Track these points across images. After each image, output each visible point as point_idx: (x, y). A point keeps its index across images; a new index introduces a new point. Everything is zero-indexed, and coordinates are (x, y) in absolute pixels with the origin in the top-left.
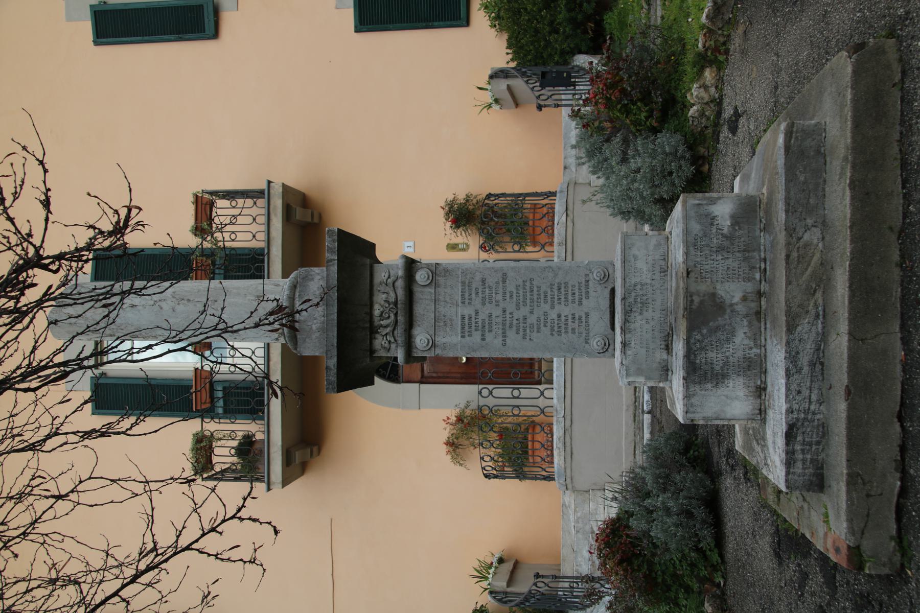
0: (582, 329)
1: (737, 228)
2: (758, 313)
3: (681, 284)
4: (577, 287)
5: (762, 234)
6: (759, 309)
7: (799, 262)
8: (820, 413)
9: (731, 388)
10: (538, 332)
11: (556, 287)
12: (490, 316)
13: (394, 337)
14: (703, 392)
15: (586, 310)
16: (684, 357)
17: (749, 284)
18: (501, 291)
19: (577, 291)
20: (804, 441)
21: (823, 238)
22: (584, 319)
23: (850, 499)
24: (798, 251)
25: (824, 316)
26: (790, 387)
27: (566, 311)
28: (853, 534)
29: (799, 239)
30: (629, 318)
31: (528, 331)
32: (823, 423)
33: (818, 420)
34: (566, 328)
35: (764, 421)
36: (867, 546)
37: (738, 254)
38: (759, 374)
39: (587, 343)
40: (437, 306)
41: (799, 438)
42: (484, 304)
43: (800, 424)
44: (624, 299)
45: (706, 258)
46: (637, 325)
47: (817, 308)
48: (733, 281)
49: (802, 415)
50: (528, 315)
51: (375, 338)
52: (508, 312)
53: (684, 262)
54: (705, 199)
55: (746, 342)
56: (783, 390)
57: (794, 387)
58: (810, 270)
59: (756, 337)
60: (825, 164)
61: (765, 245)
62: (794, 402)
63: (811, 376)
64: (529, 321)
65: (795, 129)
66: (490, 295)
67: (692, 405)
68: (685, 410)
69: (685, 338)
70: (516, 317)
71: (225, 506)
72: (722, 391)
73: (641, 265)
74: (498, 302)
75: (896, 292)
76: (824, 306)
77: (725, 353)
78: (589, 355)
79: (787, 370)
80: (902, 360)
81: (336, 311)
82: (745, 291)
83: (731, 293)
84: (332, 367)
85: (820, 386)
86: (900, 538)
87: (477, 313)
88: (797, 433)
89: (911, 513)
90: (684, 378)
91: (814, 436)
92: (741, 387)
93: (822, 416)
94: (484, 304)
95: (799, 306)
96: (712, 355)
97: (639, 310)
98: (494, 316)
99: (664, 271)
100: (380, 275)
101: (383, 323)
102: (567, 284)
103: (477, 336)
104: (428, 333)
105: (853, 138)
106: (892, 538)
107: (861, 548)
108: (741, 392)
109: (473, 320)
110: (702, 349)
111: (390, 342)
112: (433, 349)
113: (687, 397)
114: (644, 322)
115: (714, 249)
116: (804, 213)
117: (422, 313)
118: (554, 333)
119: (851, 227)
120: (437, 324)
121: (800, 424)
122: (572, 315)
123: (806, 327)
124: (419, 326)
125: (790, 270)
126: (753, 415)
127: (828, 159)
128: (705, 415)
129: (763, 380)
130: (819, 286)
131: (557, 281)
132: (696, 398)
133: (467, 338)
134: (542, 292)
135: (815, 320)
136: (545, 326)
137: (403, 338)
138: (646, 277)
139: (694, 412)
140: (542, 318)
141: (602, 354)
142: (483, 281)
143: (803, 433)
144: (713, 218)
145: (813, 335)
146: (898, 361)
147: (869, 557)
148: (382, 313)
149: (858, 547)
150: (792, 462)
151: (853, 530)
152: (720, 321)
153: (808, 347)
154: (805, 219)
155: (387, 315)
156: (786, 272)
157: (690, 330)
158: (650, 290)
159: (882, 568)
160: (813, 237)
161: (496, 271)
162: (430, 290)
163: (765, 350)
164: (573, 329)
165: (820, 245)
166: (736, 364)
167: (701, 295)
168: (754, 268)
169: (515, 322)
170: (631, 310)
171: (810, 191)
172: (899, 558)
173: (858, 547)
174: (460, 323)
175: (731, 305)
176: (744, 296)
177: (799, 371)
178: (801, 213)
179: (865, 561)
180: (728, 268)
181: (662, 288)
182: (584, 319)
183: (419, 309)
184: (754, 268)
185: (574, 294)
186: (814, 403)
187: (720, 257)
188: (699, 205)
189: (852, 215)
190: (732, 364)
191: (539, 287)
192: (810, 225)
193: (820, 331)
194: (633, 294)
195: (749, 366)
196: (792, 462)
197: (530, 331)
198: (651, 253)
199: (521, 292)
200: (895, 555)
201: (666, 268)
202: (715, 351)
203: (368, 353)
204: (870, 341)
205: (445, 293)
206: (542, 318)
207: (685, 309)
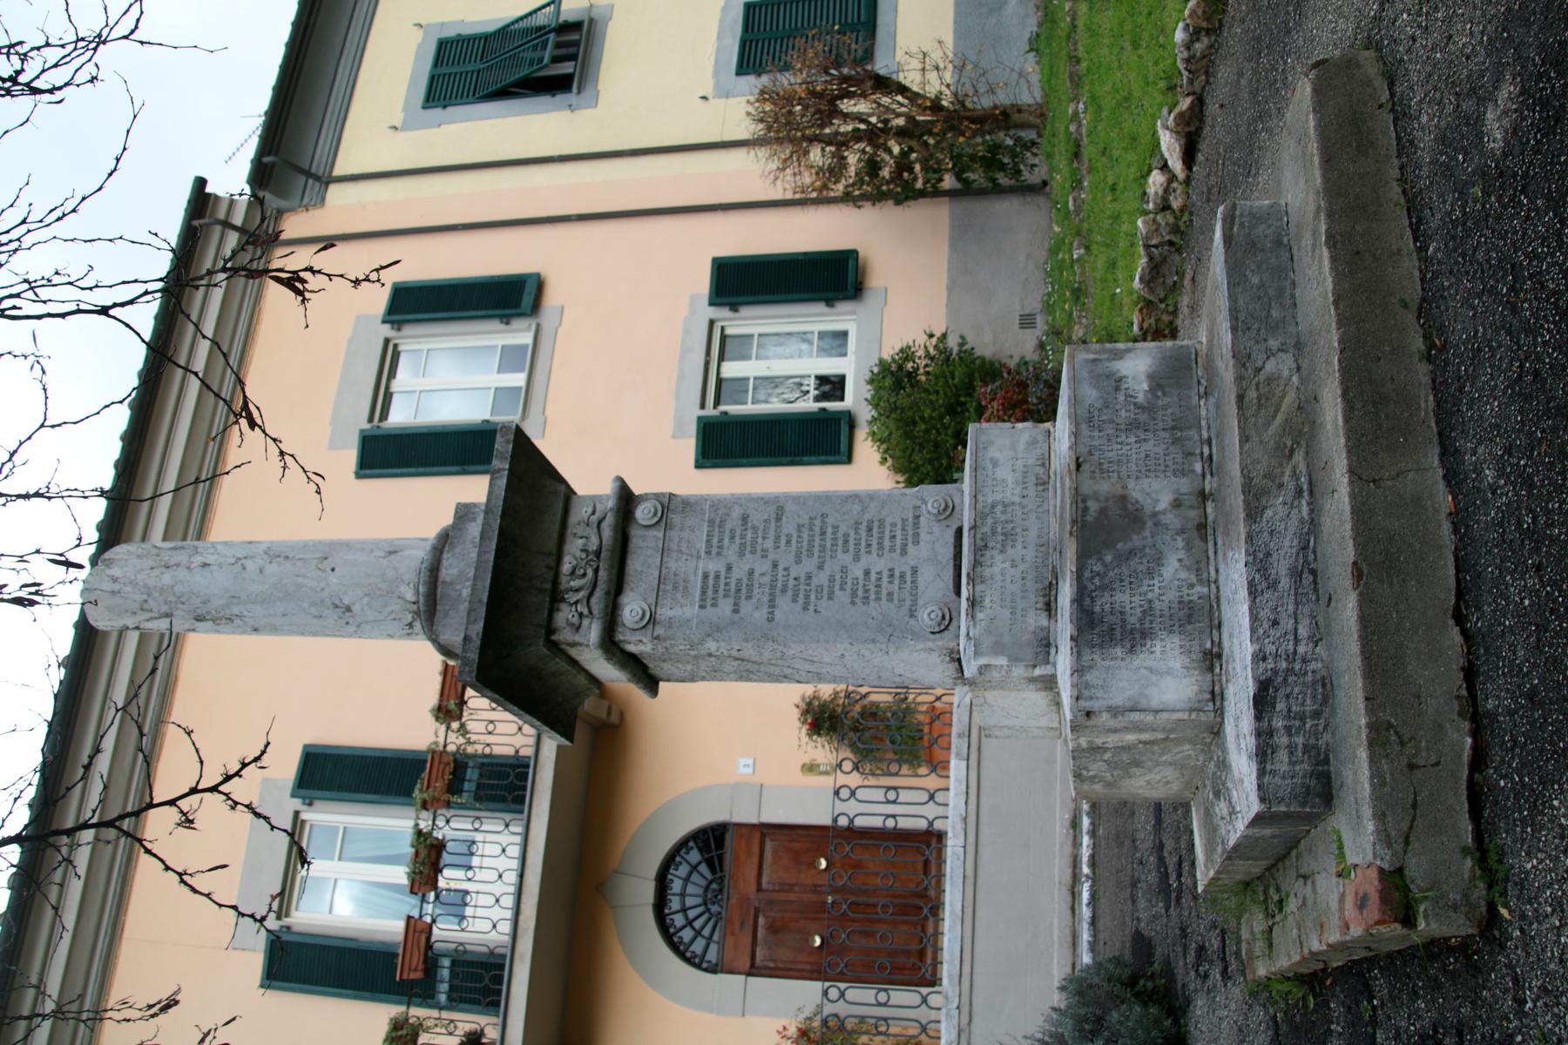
0: (906, 594)
1: (1159, 394)
2: (1202, 527)
3: (1068, 483)
4: (899, 526)
5: (1202, 403)
6: (1203, 520)
7: (1260, 406)
8: (1316, 659)
9: (1158, 653)
10: (830, 598)
11: (864, 526)
12: (751, 573)
13: (589, 608)
14: (1107, 663)
15: (913, 563)
16: (1073, 601)
17: (1184, 480)
18: (772, 534)
19: (899, 534)
20: (1289, 711)
21: (1299, 369)
22: (908, 578)
23: (1376, 773)
24: (1257, 389)
25: (1311, 493)
26: (1258, 613)
27: (879, 564)
28: (1389, 845)
29: (1259, 370)
30: (981, 559)
31: (813, 597)
32: (1323, 678)
33: (1313, 672)
34: (877, 593)
35: (1220, 712)
36: (1417, 869)
37: (1162, 434)
38: (1208, 630)
39: (912, 616)
40: (665, 559)
41: (1280, 706)
42: (742, 554)
43: (1280, 679)
44: (973, 528)
45: (1109, 441)
46: (997, 569)
47: (1298, 479)
48: (1157, 477)
49: (1284, 665)
50: (815, 571)
51: (558, 610)
52: (781, 567)
53: (1070, 448)
54: (1104, 351)
55: (1183, 575)
56: (1246, 622)
57: (1265, 613)
58: (1280, 418)
59: (1203, 567)
60: (1292, 259)
61: (1208, 419)
62: (1267, 641)
63: (1296, 594)
64: (815, 581)
65: (1238, 213)
66: (754, 541)
67: (1087, 686)
68: (1075, 694)
69: (1074, 569)
70: (793, 575)
71: (202, 762)
72: (1142, 660)
73: (1004, 473)
74: (767, 550)
75: (1426, 401)
76: (1310, 476)
77: (1145, 594)
78: (916, 636)
79: (1251, 585)
80: (1450, 514)
81: (494, 547)
82: (1177, 491)
83: (1154, 495)
84: (474, 637)
85: (1312, 611)
86: (1481, 850)
87: (729, 568)
88: (1275, 697)
89: (1497, 782)
90: (1072, 638)
91: (1308, 701)
92: (1177, 652)
93: (1320, 665)
94: (742, 554)
95: (1265, 476)
96: (1122, 598)
97: (999, 546)
98: (756, 574)
99: (1043, 483)
100: (580, 513)
101: (575, 583)
102: (882, 522)
103: (726, 606)
104: (645, 600)
105: (1324, 176)
106: (1465, 851)
107: (1407, 872)
108: (1176, 662)
109: (722, 581)
110: (1104, 587)
111: (581, 615)
112: (651, 626)
113: (1079, 670)
114: (1008, 564)
115: (1123, 427)
116: (1262, 331)
117: (639, 569)
118: (857, 600)
119: (1336, 303)
120: (662, 586)
121: (1280, 679)
122: (890, 570)
123: (1281, 511)
124: (632, 589)
125: (1246, 419)
126: (1199, 701)
127: (1295, 251)
128: (1112, 702)
129: (1216, 639)
130: (1298, 443)
131: (867, 517)
132: (1095, 673)
133: (709, 609)
134: (840, 535)
135: (1294, 498)
136: (842, 589)
137: (602, 606)
138: (1011, 493)
139: (1091, 698)
140: (838, 577)
141: (938, 636)
142: (745, 519)
143: (1288, 697)
144: (1120, 380)
145: (1293, 524)
146: (1443, 516)
147: (1422, 891)
148: (574, 569)
149: (1400, 871)
150: (1269, 751)
151: (1388, 836)
152: (1136, 540)
153: (1287, 543)
154: (1265, 340)
155: (582, 571)
156: (1239, 422)
157: (1082, 557)
158: (1019, 512)
159: (1451, 914)
160: (1280, 366)
161: (767, 503)
162: (656, 533)
163: (1218, 588)
164: (890, 594)
165: (1295, 379)
166: (1167, 613)
167: (1102, 498)
168: (1192, 454)
169: (791, 582)
170: (986, 546)
171: (1270, 299)
172: (1484, 892)
173: (1400, 871)
174: (699, 585)
175: (1155, 514)
176: (1176, 500)
177: (1273, 586)
178: (1259, 330)
179: (1416, 900)
180: (1147, 456)
181: (1040, 510)
182: (908, 578)
183: (634, 564)
184: (1192, 454)
185: (893, 537)
186: (1304, 642)
187: (1133, 439)
188: (1095, 360)
189: (1336, 284)
190: (1158, 613)
191: (836, 528)
192: (1275, 348)
193: (1306, 517)
194: (990, 521)
195: (1190, 616)
196: (1269, 751)
197: (816, 597)
198: (1021, 455)
199: (805, 536)
200: (1475, 887)
201: (1046, 478)
202: (1128, 591)
203: (543, 631)
204: (1389, 483)
205: (681, 539)
206: (838, 577)
207: (1074, 522)
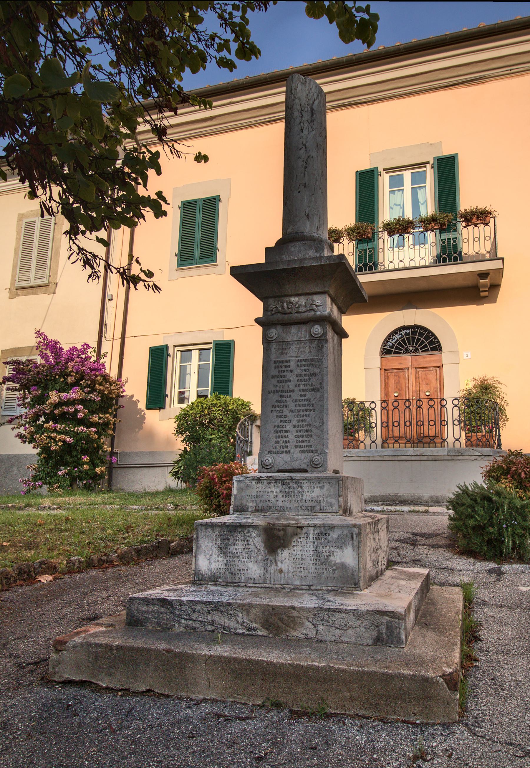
0: (278, 449)
4: (308, 444)
9: (217, 559)
10: (277, 416)
12: (289, 381)
15: (292, 451)
16: (240, 523)
19: (305, 444)
22: (285, 449)
25: (249, 635)
27: (291, 436)
30: (278, 482)
31: (278, 409)
34: (279, 436)
39: (269, 452)
40: (296, 342)
44: (292, 479)
46: (273, 489)
50: (289, 409)
52: (291, 394)
57: (198, 607)
64: (285, 409)
66: (303, 380)
72: (215, 551)
74: (299, 387)
87: (291, 371)
94: (297, 376)
98: (289, 383)
102: (311, 436)
108: (214, 566)
111: (272, 310)
124: (283, 330)
131: (313, 429)
133: (273, 366)
134: (305, 418)
136: (281, 421)
140: (286, 419)
142: (314, 375)
145: (233, 625)
148: (292, 303)
161: (321, 383)
166: (234, 563)
174: (284, 359)
175: (276, 562)
182: (285, 449)
191: (308, 416)
195: (232, 573)
198: (325, 500)
